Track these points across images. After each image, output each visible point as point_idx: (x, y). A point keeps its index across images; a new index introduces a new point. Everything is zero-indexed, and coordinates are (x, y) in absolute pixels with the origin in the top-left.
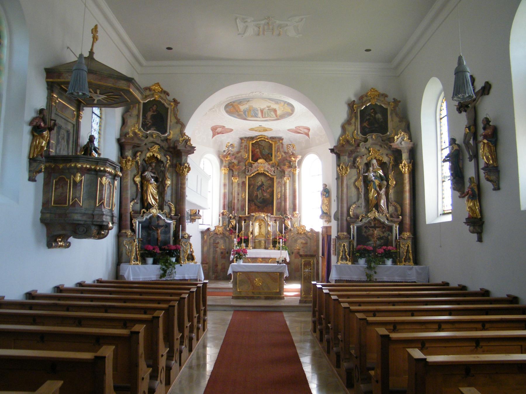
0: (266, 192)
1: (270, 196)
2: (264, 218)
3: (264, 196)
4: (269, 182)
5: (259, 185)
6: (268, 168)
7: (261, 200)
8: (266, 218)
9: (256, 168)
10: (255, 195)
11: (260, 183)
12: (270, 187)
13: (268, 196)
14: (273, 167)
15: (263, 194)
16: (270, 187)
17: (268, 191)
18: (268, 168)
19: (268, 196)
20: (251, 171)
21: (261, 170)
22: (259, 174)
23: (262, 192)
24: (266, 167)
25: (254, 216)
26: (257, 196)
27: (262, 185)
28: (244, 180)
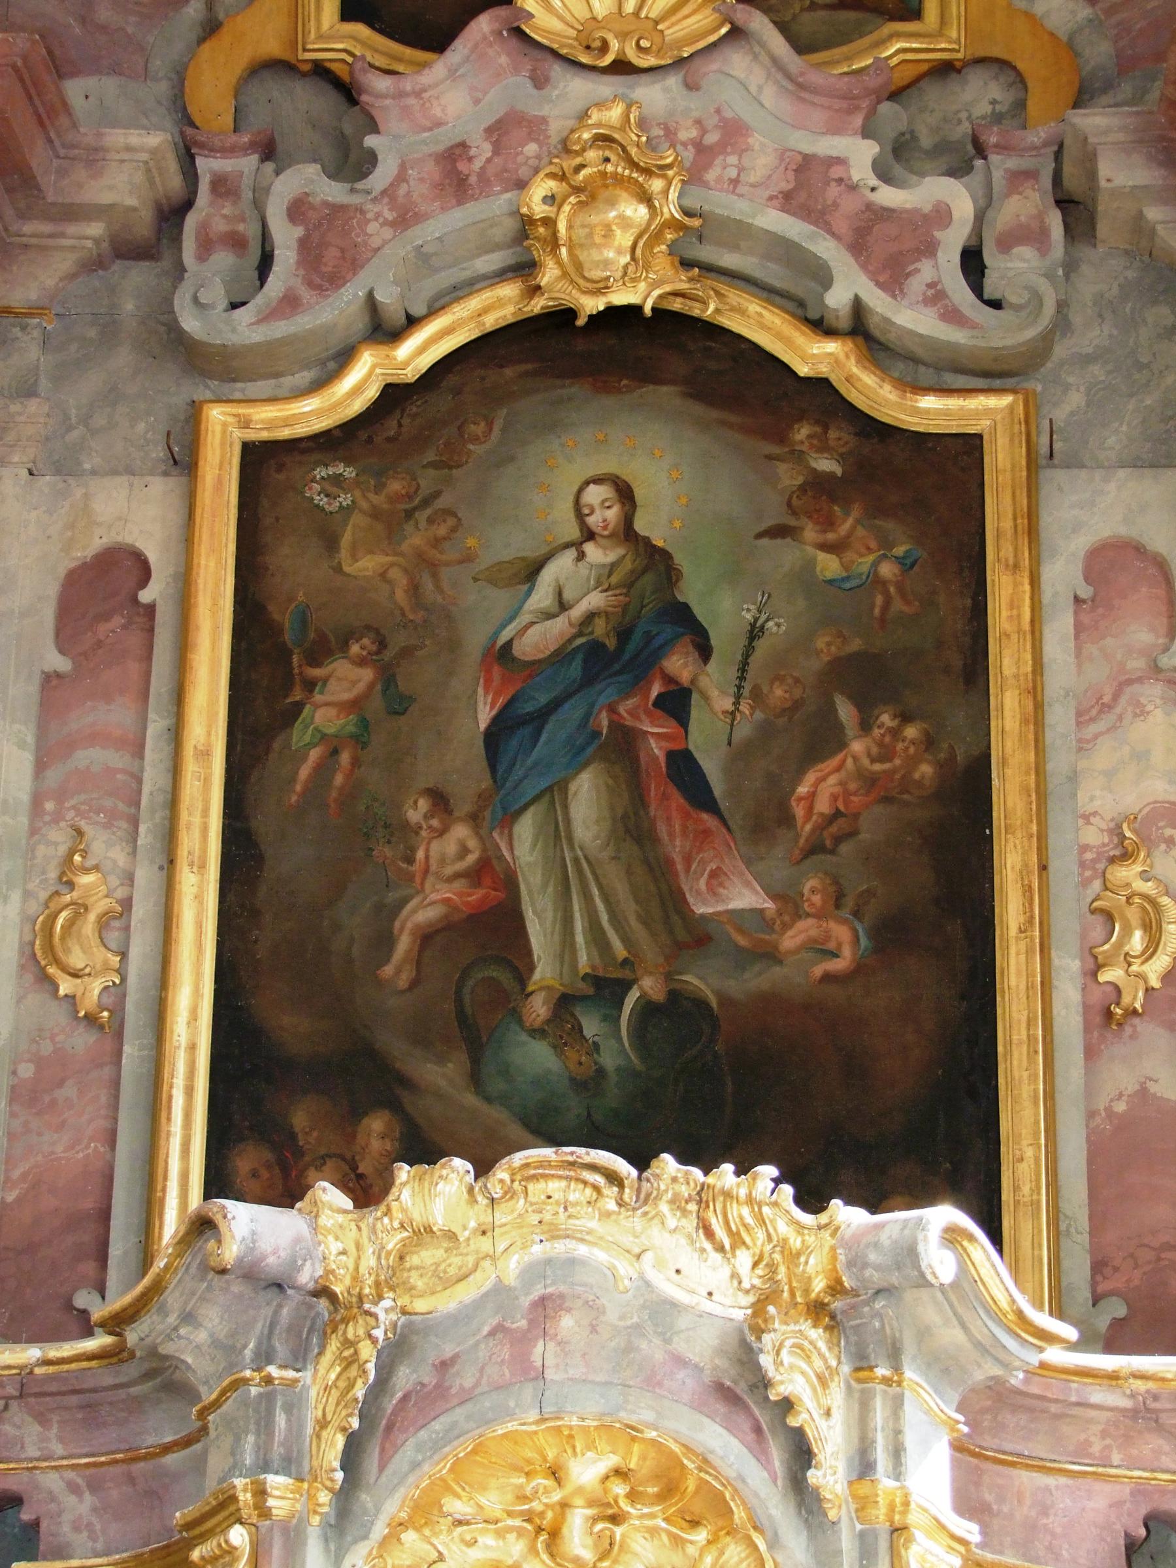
0: (770, 819)
1: (891, 935)
2: (743, 1390)
3: (694, 938)
4: (865, 555)
5: (538, 638)
6: (807, 186)
7: (611, 1042)
8: (799, 1365)
9: (455, 176)
10: (422, 912)
11: (576, 588)
12: (869, 678)
13: (823, 944)
14: (964, 156)
15: (667, 904)
16: (869, 678)
17: (820, 789)
18: (807, 186)
19: (823, 944)
20: (330, 251)
21: (614, 260)
22: (573, 353)
23: (633, 829)
24: (761, 161)
25: (324, 1311)
26: (492, 928)
27: (649, 624)
28: (135, 514)
